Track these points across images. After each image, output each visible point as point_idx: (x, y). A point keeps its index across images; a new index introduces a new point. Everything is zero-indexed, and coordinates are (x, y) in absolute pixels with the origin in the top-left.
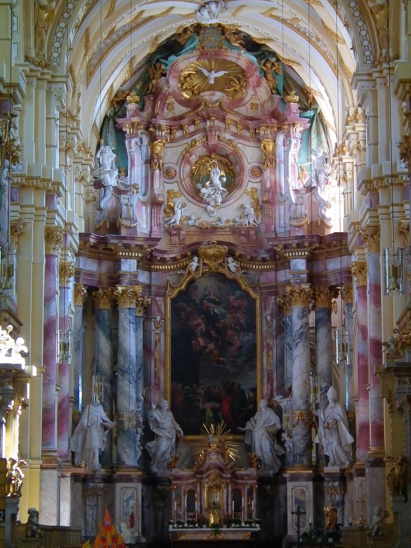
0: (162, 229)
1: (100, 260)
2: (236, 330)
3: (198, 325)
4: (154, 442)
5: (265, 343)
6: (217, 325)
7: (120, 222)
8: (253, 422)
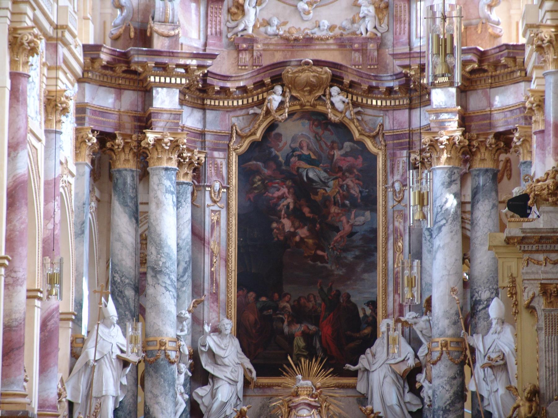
0: (224, 40)
1: (119, 89)
2: (344, 205)
3: (282, 197)
4: (207, 388)
5: (391, 227)
6: (312, 197)
7: (151, 28)
8: (370, 356)
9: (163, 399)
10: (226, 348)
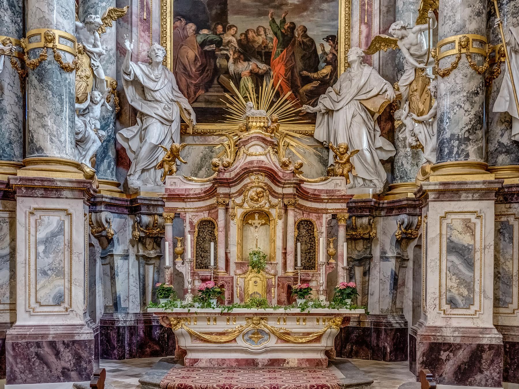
8: (333, 95)
9: (52, 120)
10: (157, 80)
